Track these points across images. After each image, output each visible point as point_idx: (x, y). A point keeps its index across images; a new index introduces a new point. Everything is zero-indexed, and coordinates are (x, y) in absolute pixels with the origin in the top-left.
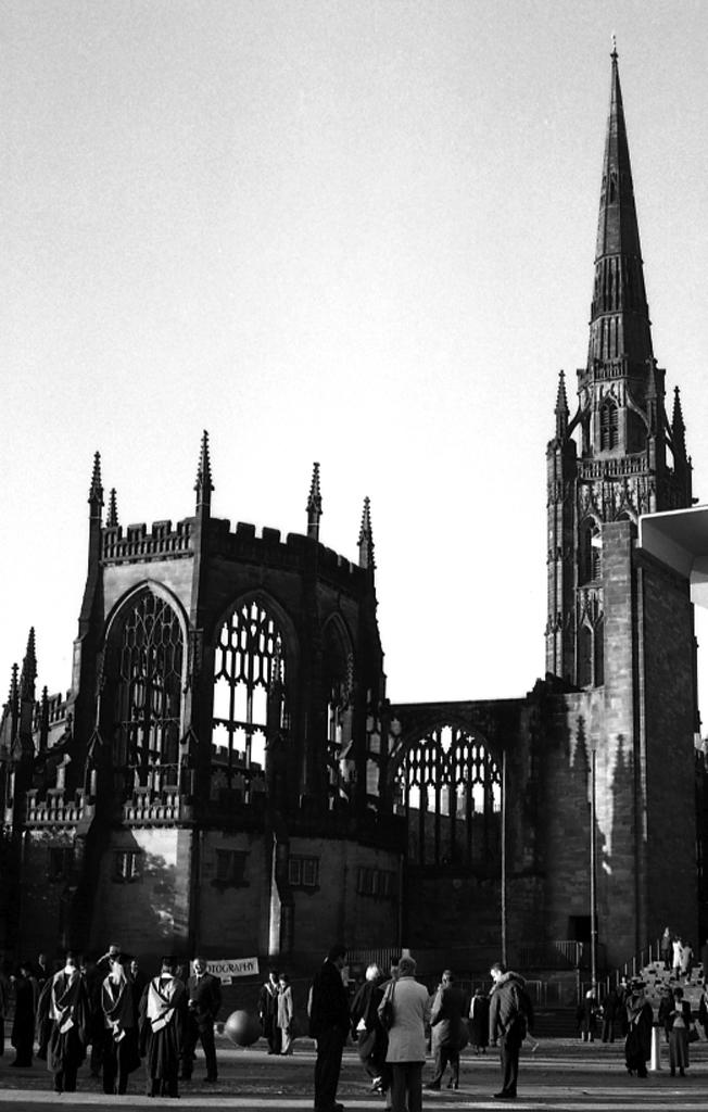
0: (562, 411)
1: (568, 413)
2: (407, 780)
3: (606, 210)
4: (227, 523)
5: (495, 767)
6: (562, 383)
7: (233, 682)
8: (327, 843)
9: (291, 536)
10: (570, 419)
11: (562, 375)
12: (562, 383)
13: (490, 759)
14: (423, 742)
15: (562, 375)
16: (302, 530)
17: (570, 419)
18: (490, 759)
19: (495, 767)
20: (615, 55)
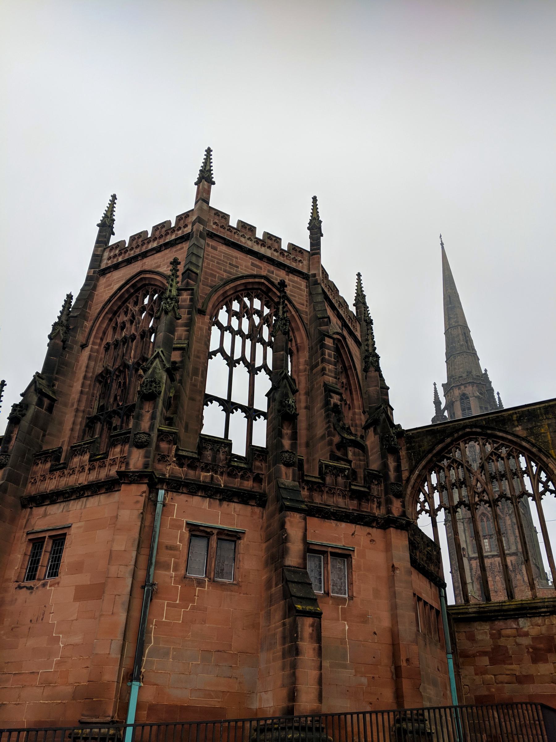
0: (437, 402)
1: (440, 403)
2: (432, 505)
3: (448, 308)
4: (226, 217)
5: (543, 476)
6: (435, 388)
7: (231, 363)
8: (361, 531)
9: (293, 247)
10: (443, 406)
11: (435, 384)
12: (435, 388)
13: (535, 469)
14: (445, 462)
15: (435, 384)
16: (305, 244)
17: (443, 406)
18: (535, 469)
19: (543, 476)
20: (442, 244)
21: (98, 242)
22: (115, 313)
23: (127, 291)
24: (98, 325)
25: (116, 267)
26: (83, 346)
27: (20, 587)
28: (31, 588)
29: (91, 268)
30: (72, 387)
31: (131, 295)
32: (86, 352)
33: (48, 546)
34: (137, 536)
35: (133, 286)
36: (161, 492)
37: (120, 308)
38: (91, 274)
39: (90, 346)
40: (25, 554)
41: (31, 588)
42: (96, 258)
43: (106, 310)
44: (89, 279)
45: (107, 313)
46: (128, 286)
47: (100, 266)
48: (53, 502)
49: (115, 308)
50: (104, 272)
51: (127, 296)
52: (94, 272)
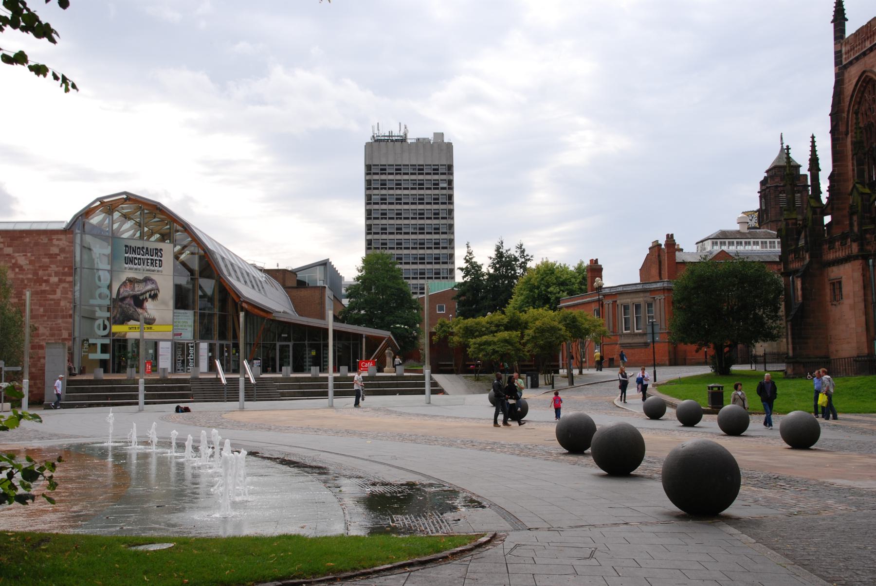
21: (836, 38)
22: (859, 103)
23: (861, 85)
24: (850, 116)
25: (851, 63)
26: (847, 134)
27: (832, 305)
28: (835, 305)
29: (836, 64)
30: (847, 166)
31: (865, 88)
32: (849, 140)
33: (837, 286)
34: (862, 284)
35: (863, 81)
36: (871, 261)
37: (861, 98)
38: (837, 71)
39: (850, 134)
40: (830, 290)
41: (835, 305)
42: (838, 55)
43: (853, 103)
44: (837, 75)
45: (854, 106)
46: (860, 83)
47: (841, 61)
48: (834, 265)
49: (858, 100)
50: (845, 67)
51: (862, 89)
52: (840, 69)
